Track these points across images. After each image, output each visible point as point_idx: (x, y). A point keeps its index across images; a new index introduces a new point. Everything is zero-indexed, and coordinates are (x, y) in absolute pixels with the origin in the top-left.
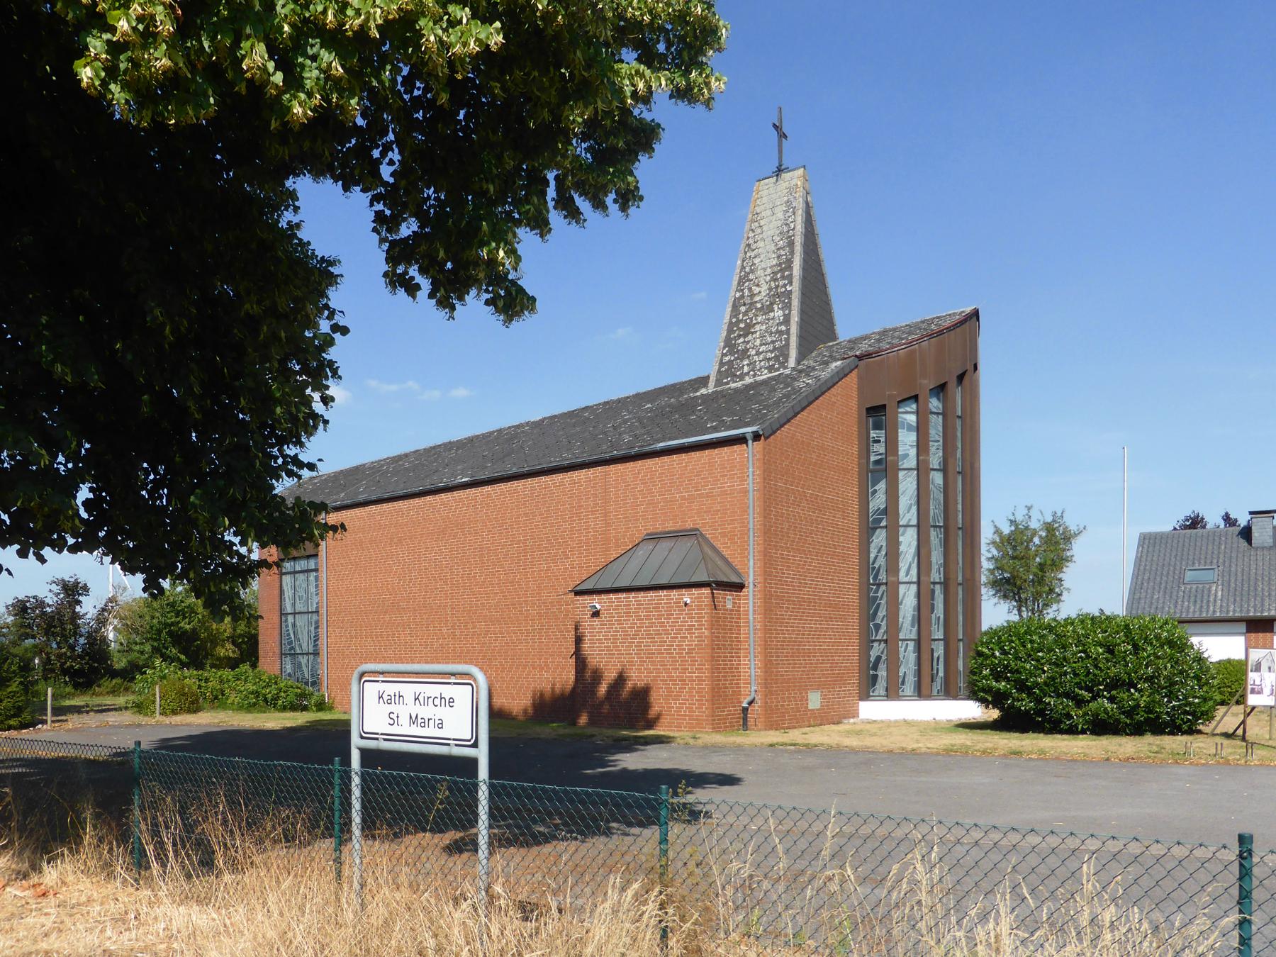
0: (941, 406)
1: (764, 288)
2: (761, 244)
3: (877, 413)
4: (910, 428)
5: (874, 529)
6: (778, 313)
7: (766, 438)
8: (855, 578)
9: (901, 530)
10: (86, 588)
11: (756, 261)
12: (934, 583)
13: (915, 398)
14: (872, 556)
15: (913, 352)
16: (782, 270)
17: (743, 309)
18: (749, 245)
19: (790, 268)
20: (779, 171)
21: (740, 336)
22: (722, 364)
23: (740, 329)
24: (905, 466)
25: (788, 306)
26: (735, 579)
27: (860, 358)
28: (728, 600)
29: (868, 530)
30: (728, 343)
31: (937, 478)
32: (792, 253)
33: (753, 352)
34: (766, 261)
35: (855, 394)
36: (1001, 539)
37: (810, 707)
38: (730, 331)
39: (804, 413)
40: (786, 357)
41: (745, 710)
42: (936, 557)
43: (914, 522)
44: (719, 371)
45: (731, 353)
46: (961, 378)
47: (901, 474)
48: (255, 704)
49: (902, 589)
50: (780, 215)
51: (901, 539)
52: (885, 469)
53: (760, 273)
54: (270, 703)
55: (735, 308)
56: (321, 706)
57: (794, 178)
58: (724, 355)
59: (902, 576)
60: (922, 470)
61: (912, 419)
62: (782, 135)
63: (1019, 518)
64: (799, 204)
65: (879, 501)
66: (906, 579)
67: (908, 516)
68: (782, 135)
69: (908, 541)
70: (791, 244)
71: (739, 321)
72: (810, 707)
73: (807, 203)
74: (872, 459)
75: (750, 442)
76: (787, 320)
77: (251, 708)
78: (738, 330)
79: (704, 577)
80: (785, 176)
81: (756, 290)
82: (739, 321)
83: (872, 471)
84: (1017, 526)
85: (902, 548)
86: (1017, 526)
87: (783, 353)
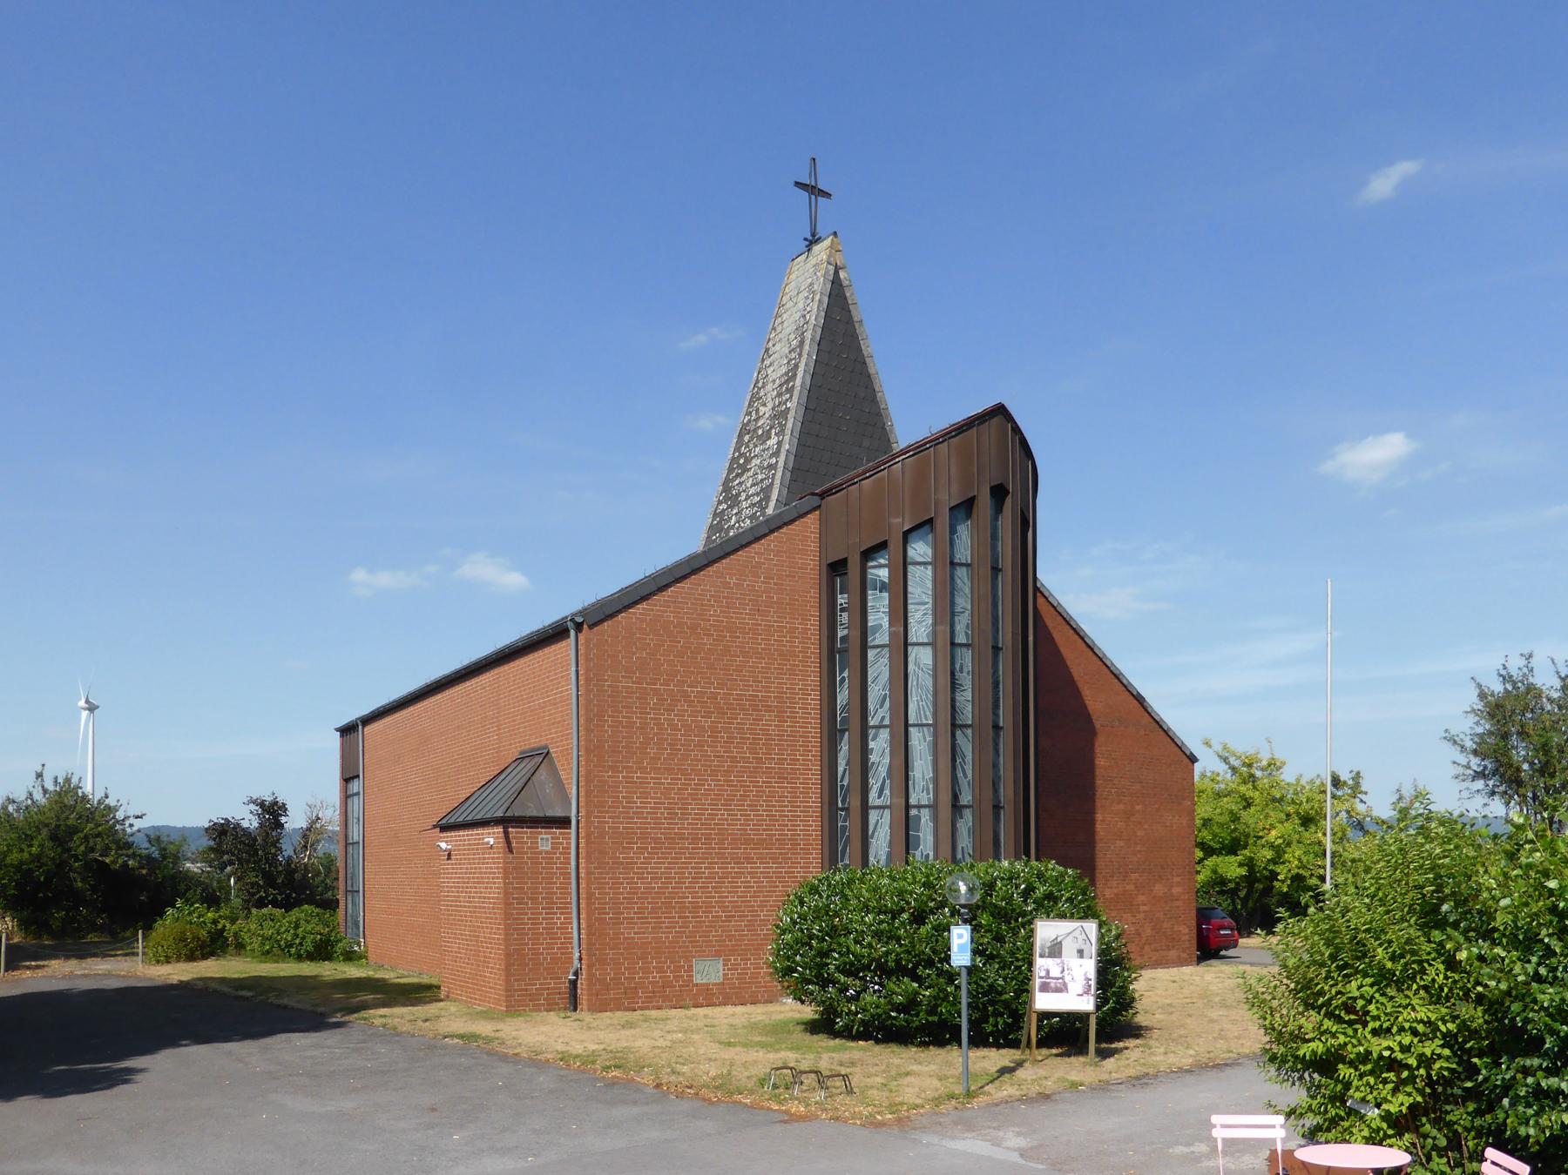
0: (929, 552)
1: (770, 405)
2: (778, 347)
3: (837, 568)
4: (883, 587)
5: (843, 731)
6: (773, 441)
7: (591, 627)
8: (814, 801)
9: (872, 732)
10: (283, 808)
11: (770, 371)
12: (919, 807)
13: (883, 546)
14: (840, 769)
15: (882, 479)
16: (787, 382)
17: (746, 438)
18: (767, 350)
19: (795, 375)
20: (813, 241)
21: (738, 475)
22: (715, 515)
23: (739, 466)
24: (877, 642)
25: (782, 432)
26: (558, 812)
27: (822, 495)
28: (545, 840)
29: (832, 736)
30: (727, 487)
31: (922, 659)
32: (800, 355)
33: (743, 496)
34: (776, 372)
35: (813, 546)
36: (1487, 705)
37: (698, 979)
38: (731, 470)
39: (685, 585)
40: (767, 499)
41: (574, 983)
42: (922, 768)
43: (887, 722)
44: (711, 526)
45: (726, 500)
46: (966, 507)
47: (871, 654)
48: (268, 952)
49: (873, 816)
50: (801, 305)
51: (872, 745)
52: (842, 653)
53: (769, 387)
54: (285, 951)
55: (740, 436)
56: (350, 957)
57: (821, 251)
58: (720, 503)
59: (873, 798)
60: (901, 645)
61: (884, 574)
62: (814, 191)
63: (1514, 672)
64: (821, 286)
65: (842, 697)
66: (878, 802)
67: (881, 713)
68: (814, 191)
69: (880, 745)
70: (802, 343)
71: (741, 455)
72: (698, 979)
73: (836, 283)
74: (840, 634)
75: (572, 633)
76: (776, 454)
77: (266, 955)
78: (738, 466)
79: (499, 814)
80: (816, 248)
81: (762, 409)
82: (741, 455)
83: (841, 652)
84: (1514, 683)
85: (873, 758)
86: (1514, 683)
87: (766, 492)
